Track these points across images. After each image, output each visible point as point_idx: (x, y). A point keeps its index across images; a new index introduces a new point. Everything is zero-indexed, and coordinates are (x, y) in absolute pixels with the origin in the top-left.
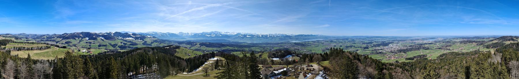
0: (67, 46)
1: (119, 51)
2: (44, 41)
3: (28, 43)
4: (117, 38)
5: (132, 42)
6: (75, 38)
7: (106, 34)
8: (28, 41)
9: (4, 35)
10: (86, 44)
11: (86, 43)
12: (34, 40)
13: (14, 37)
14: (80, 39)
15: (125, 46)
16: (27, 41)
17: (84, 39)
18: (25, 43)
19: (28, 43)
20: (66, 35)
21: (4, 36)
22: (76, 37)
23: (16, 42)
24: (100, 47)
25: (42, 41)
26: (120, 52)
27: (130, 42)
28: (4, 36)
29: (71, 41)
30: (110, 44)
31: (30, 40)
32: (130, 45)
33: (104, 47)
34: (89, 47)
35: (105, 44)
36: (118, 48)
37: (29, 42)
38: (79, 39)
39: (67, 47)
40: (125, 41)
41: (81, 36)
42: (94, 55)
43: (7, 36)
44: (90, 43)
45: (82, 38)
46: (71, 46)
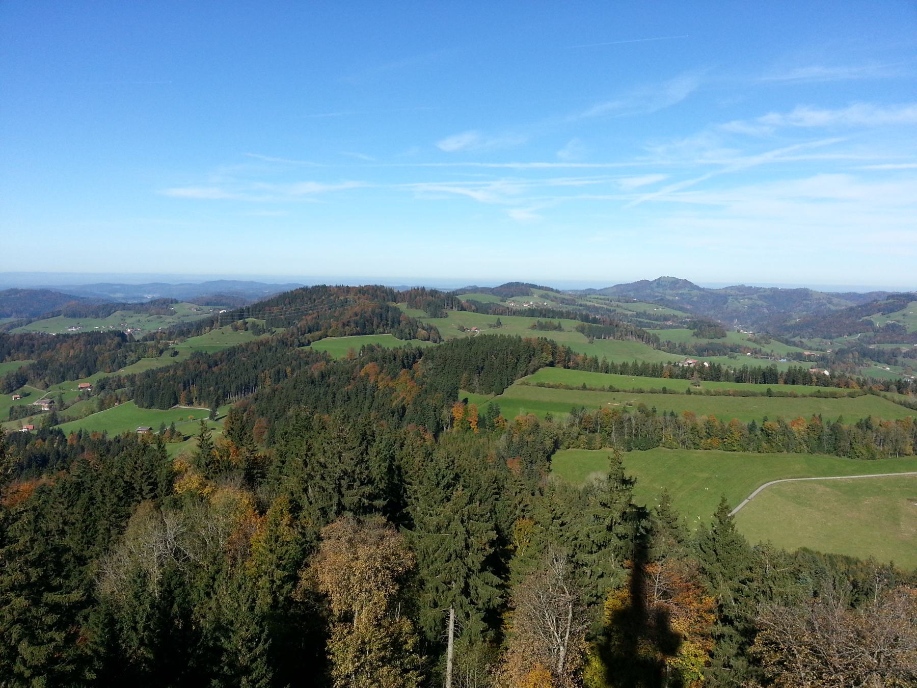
2: (890, 359)
3: (715, 374)
8: (717, 359)
9: (484, 299)
12: (780, 349)
13: (568, 315)
16: (701, 351)
18: (685, 374)
19: (715, 374)
21: (480, 308)
23: (594, 365)
25: (878, 357)
28: (480, 308)
31: (735, 349)
37: (725, 362)
43: (511, 304)
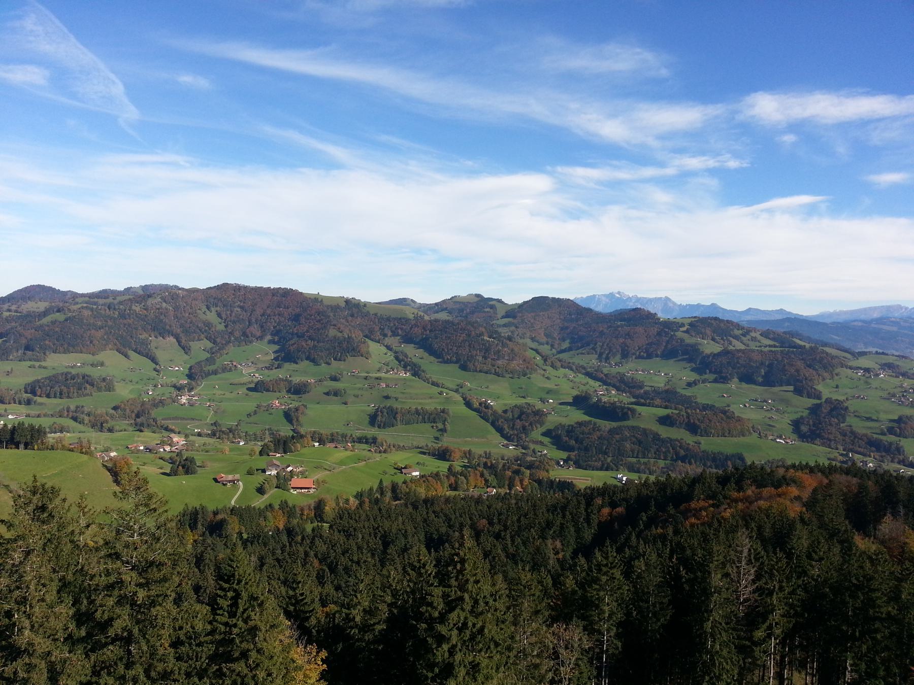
0: (45, 422)
1: (560, 474)
4: (545, 349)
5: (688, 402)
6: (145, 343)
7: (443, 316)
10: (251, 406)
11: (258, 387)
14: (200, 348)
15: (612, 431)
17: (233, 353)
20: (42, 306)
22: (161, 331)
24: (382, 435)
26: (565, 486)
27: (668, 396)
29: (96, 373)
30: (483, 411)
32: (665, 421)
33: (424, 435)
34: (286, 431)
35: (431, 406)
36: (549, 452)
38: (186, 349)
39: (51, 438)
40: (624, 384)
41: (208, 325)
42: (329, 509)
44: (298, 390)
45: (218, 343)
46: (99, 425)
